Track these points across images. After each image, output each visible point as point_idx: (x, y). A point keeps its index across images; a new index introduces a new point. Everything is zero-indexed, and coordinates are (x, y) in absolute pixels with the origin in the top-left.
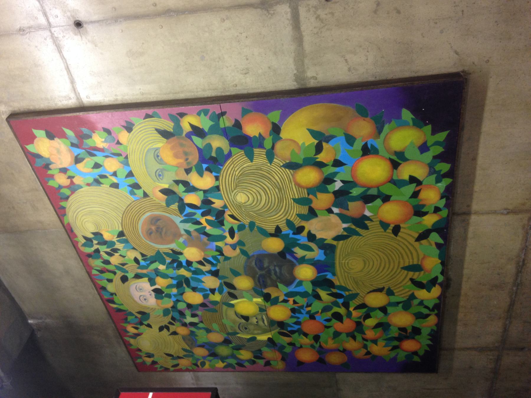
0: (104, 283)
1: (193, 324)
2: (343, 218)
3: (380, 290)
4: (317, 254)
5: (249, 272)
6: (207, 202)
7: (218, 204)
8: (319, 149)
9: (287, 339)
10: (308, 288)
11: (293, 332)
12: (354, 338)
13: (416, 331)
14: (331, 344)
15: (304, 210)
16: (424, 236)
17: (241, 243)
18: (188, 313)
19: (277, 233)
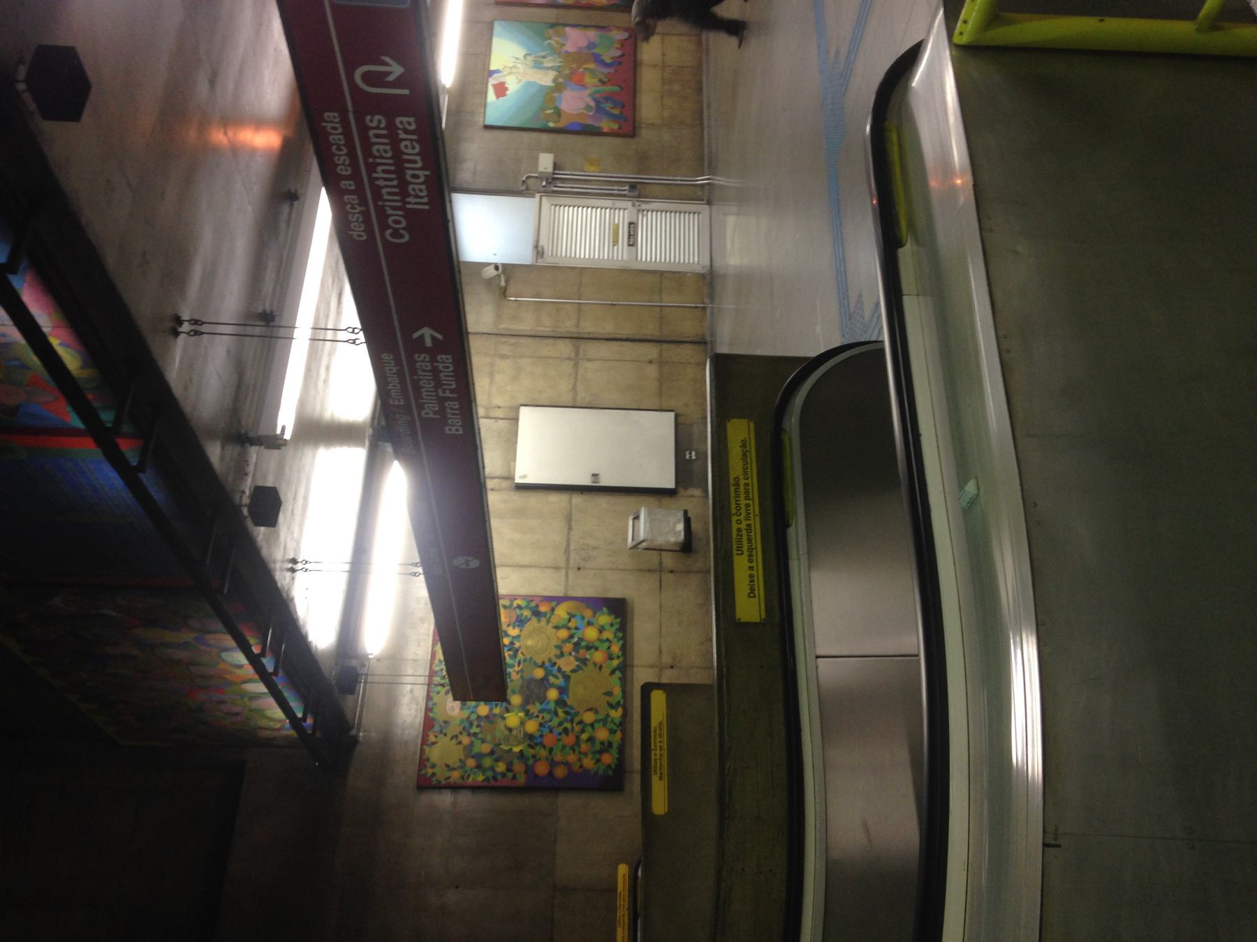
0: (432, 694)
1: (475, 734)
2: (577, 659)
3: (590, 709)
4: (560, 681)
5: (521, 693)
6: (512, 643)
7: (517, 645)
8: (569, 621)
9: (532, 751)
10: (552, 706)
11: (537, 744)
12: (574, 750)
13: (610, 744)
14: (558, 757)
15: (558, 652)
16: (613, 672)
17: (522, 671)
18: (475, 723)
19: (543, 666)
